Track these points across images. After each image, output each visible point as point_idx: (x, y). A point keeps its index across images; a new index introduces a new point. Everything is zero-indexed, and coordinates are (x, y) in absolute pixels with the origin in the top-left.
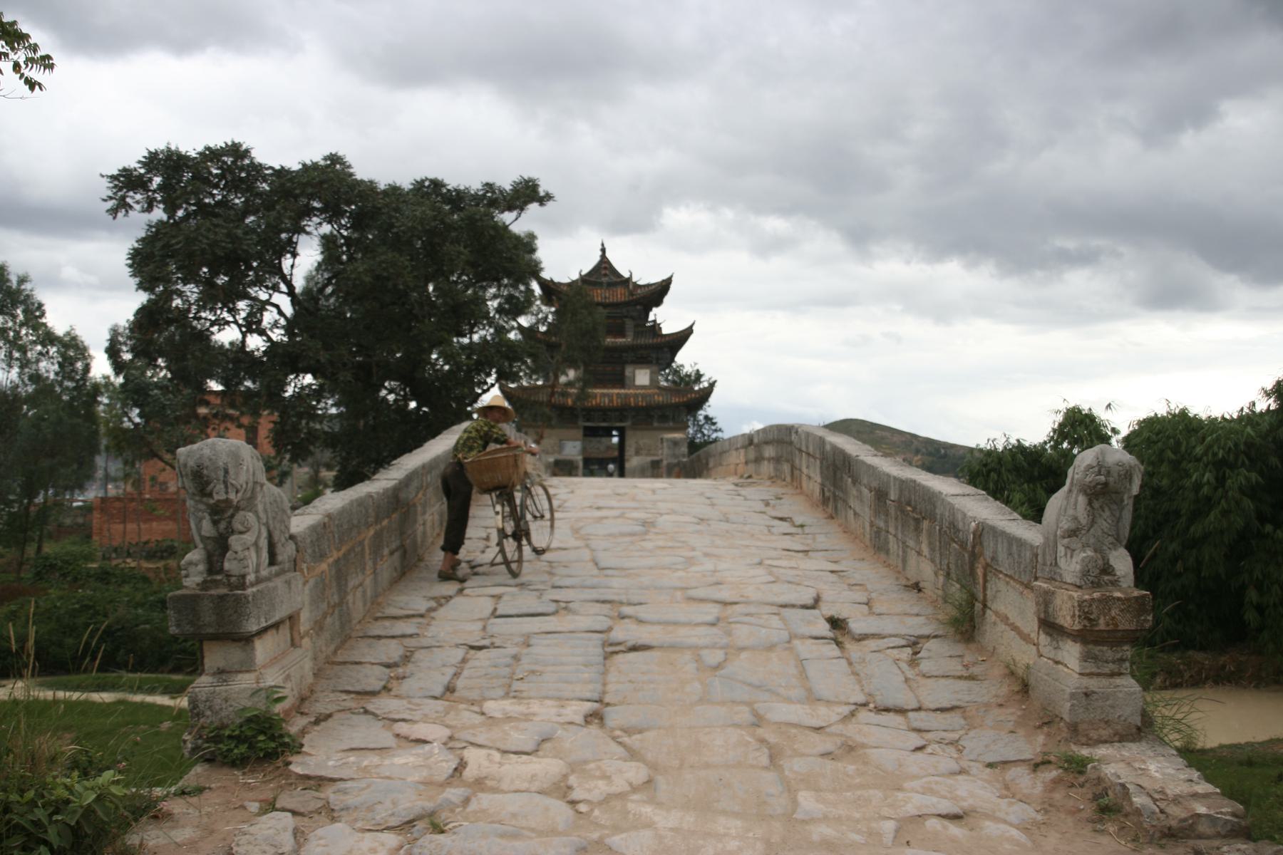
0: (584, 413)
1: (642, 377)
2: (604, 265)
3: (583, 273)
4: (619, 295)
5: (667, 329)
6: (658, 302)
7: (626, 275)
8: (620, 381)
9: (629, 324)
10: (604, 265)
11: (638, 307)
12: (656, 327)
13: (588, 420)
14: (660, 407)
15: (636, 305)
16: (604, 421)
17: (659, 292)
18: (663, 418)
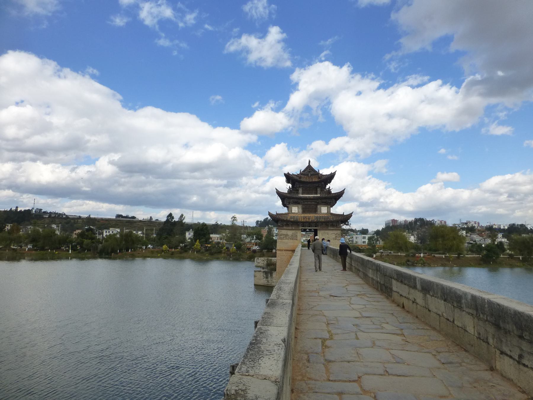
0: (302, 224)
1: (324, 210)
2: (309, 168)
3: (301, 171)
4: (315, 180)
5: (333, 192)
6: (330, 182)
7: (318, 171)
8: (315, 211)
9: (319, 190)
10: (309, 168)
11: (322, 183)
12: (329, 191)
13: (303, 227)
14: (331, 222)
15: (321, 182)
16: (309, 227)
17: (331, 177)
18: (333, 226)
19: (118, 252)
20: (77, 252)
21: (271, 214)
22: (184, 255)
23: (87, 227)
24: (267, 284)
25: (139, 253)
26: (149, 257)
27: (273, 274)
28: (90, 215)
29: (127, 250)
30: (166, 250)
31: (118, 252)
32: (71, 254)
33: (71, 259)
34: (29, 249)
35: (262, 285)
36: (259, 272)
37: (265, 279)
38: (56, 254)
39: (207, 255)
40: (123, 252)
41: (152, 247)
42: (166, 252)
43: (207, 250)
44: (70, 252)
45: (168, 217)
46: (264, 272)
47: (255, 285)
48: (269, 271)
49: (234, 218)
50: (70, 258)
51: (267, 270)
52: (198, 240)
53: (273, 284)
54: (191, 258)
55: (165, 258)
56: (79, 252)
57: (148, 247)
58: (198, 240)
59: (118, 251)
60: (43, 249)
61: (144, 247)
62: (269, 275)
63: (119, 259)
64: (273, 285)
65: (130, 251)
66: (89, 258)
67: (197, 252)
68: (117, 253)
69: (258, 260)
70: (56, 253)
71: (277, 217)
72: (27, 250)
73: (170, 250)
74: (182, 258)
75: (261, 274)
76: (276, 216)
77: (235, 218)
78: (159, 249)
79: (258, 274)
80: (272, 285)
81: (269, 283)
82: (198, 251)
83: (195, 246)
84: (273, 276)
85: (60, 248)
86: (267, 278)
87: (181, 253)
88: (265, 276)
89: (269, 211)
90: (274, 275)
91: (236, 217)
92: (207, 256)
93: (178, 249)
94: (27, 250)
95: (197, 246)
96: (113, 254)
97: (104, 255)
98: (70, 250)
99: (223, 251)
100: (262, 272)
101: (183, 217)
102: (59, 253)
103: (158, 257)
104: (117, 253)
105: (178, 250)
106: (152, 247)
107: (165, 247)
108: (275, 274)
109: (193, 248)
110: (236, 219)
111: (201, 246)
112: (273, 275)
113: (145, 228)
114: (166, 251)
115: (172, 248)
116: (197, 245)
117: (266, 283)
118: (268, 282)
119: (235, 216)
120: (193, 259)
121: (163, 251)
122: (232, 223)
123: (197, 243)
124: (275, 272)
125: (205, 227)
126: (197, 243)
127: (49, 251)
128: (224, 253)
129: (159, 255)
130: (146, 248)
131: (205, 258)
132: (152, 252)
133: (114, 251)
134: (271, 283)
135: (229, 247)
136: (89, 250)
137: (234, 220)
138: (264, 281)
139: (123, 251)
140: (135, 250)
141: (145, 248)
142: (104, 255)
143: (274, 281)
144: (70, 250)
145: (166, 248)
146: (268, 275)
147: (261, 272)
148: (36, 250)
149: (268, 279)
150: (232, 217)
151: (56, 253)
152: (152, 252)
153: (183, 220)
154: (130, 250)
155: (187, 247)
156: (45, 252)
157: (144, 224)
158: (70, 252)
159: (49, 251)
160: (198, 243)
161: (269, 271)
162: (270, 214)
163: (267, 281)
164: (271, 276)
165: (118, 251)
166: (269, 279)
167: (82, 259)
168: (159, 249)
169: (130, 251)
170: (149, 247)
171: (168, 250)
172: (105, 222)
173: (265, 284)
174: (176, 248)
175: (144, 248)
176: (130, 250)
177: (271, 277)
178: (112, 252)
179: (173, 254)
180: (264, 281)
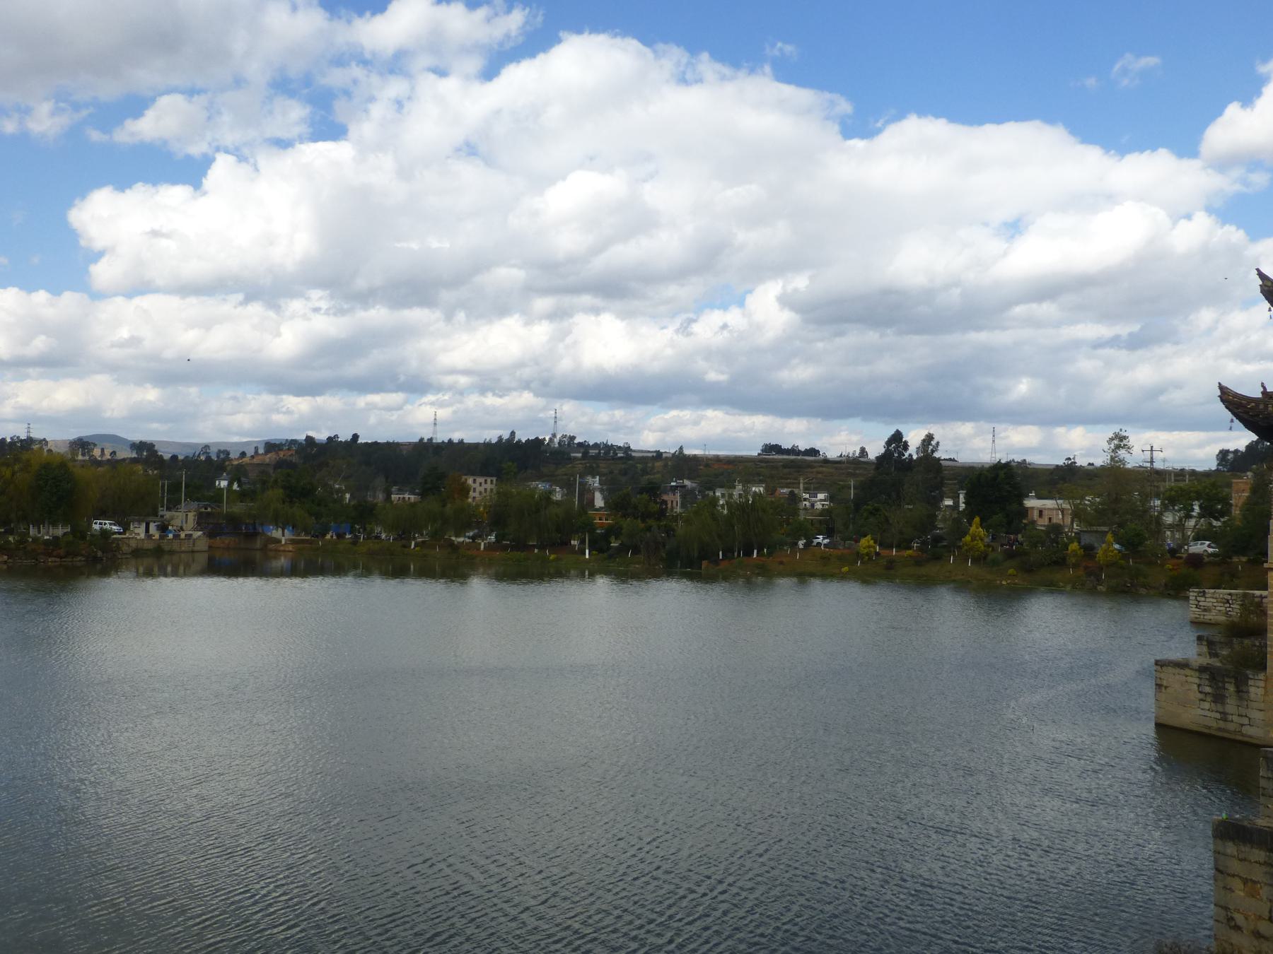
19: (721, 557)
20: (605, 555)
21: (1236, 395)
22: (932, 569)
23: (676, 481)
24: (1219, 729)
25: (781, 563)
26: (813, 575)
27: (1251, 682)
28: (681, 448)
29: (748, 553)
30: (867, 554)
31: (721, 557)
32: (588, 561)
33: (592, 575)
34: (490, 547)
35: (1195, 728)
36: (1177, 670)
37: (1206, 705)
38: (553, 561)
39: (1011, 571)
40: (733, 558)
41: (826, 541)
42: (870, 559)
43: (1010, 555)
44: (587, 557)
45: (889, 443)
46: (1202, 669)
47: (1160, 727)
48: (1229, 667)
49: (1120, 441)
50: (587, 573)
51: (1219, 664)
52: (977, 519)
53: (1249, 731)
54: (954, 581)
55: (866, 579)
56: (611, 557)
57: (816, 541)
58: (977, 519)
59: (721, 553)
60: (520, 545)
61: (801, 543)
62: (1231, 688)
63: (725, 579)
64: (1250, 737)
65: (755, 556)
66: (638, 576)
67: (975, 561)
68: (716, 562)
69: (1203, 599)
70: (552, 557)
71: (1266, 406)
72: (482, 547)
73: (885, 552)
74: (924, 583)
75: (1190, 679)
76: (1261, 407)
77: (1122, 438)
78: (849, 548)
79: (1173, 679)
80: (1243, 735)
81: (1231, 727)
82: (980, 559)
83: (968, 538)
84: (1252, 696)
85: (567, 543)
86: (1219, 698)
87: (918, 563)
88: (1208, 689)
89: (1224, 384)
90: (1256, 689)
91: (1125, 438)
92: (1010, 575)
93: (910, 548)
94: (482, 547)
95: (975, 540)
96: (705, 563)
97: (681, 568)
98: (587, 551)
99: (1073, 560)
100: (1196, 670)
101: (933, 443)
102: (557, 560)
103: (843, 577)
104: (716, 562)
105: (909, 552)
106: (826, 541)
107: (866, 542)
108: (1262, 684)
109: (960, 548)
110: (1125, 442)
111: (993, 539)
112: (1252, 690)
113: (801, 481)
114: (867, 557)
115: (890, 547)
116: (973, 539)
117: (1214, 724)
118: (1225, 720)
119: (1124, 434)
120: (961, 586)
121: (859, 556)
122: (1112, 459)
123: (976, 528)
124: (1261, 676)
125: (1002, 474)
126: (973, 529)
127: (536, 551)
128: (1075, 566)
129: (845, 569)
130: (807, 545)
131: (1004, 583)
132: (825, 559)
133: (706, 554)
134: (1242, 725)
135: (1096, 545)
136: (636, 551)
137: (1118, 447)
138: (1203, 712)
139: (736, 554)
140: (770, 554)
141: (805, 545)
142: (679, 565)
143: (1256, 715)
144: (587, 551)
145: (869, 547)
146: (1225, 689)
147: (1188, 672)
148: (505, 548)
149: (1223, 704)
150: (1111, 435)
151: (552, 557)
152: (823, 558)
153: (933, 451)
154: (755, 551)
155: (940, 544)
156: (523, 555)
157: (836, 469)
158: (587, 557)
159: (536, 551)
160: (977, 528)
161: (1229, 667)
162: (1235, 403)
163: (1218, 716)
164: (1238, 691)
165: (721, 553)
166: (1231, 706)
167: (623, 576)
168: (849, 548)
169: (755, 556)
170: (819, 544)
171: (877, 554)
172: (725, 467)
173: (1210, 728)
174: (904, 544)
175: (801, 547)
176: (755, 551)
177: (1241, 698)
178: (702, 557)
179: (891, 565)
180: (1203, 712)
